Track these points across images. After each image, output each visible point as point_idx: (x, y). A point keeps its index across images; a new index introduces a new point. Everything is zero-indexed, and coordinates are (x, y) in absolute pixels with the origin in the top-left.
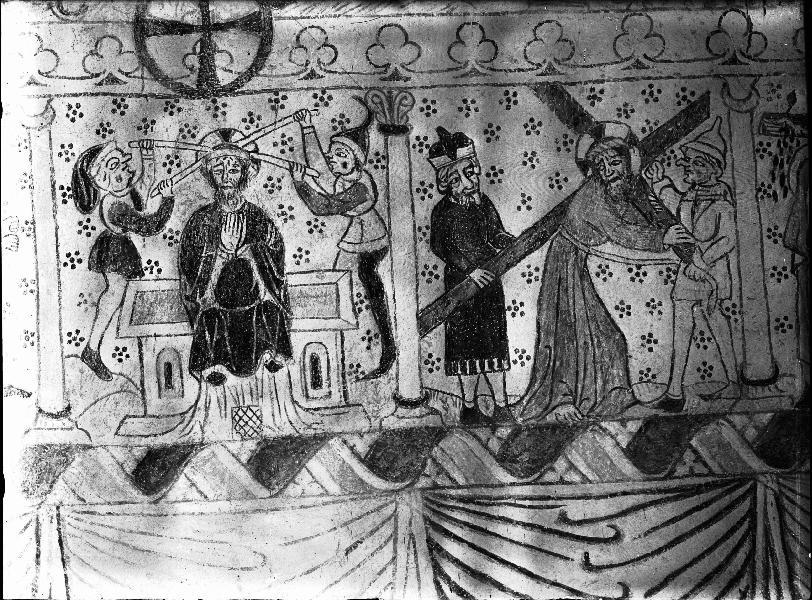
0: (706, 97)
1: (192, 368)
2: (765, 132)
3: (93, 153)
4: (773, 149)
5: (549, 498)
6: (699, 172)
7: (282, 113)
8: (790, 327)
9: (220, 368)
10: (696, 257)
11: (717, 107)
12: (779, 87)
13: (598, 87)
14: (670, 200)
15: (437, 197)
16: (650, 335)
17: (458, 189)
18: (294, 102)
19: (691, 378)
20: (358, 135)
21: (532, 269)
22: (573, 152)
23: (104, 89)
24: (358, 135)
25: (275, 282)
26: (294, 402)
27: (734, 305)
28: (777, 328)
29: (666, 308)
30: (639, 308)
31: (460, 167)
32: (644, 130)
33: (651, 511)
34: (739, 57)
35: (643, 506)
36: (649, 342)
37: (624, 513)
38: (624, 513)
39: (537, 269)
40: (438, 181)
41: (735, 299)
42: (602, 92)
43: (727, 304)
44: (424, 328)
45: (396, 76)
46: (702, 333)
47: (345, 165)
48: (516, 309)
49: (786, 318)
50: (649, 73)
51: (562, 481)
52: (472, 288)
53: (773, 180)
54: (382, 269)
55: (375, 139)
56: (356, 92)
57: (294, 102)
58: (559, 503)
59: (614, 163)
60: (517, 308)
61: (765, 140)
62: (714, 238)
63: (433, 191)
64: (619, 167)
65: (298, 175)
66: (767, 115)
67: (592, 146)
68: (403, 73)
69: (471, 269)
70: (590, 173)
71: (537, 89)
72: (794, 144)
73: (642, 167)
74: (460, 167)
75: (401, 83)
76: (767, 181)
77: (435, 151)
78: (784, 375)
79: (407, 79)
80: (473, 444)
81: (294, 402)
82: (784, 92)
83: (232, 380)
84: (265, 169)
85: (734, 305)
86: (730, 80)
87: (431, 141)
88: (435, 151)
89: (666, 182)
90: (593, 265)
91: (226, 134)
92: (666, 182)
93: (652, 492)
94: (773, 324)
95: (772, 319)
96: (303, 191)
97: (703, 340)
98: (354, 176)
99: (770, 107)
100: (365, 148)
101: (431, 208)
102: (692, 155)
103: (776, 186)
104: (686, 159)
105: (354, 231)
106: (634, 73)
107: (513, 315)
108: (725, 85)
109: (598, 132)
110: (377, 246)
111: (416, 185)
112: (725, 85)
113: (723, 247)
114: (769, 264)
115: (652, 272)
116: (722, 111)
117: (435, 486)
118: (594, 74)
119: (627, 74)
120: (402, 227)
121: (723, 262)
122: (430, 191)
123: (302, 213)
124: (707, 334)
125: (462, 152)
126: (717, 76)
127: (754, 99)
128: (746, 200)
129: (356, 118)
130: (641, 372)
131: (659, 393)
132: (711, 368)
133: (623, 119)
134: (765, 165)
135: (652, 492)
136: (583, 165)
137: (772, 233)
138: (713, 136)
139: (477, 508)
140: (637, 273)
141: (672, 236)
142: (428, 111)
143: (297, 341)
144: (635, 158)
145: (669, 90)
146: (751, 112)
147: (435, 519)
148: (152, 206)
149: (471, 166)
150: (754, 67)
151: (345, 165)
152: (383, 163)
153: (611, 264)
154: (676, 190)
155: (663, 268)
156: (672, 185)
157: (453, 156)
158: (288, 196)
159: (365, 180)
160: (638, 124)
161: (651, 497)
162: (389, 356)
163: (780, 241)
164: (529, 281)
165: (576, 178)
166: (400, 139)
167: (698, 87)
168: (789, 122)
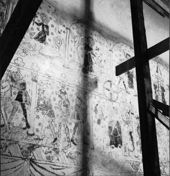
1: (110, 145)
3: (97, 105)
9: (113, 146)
20: (129, 113)
23: (99, 95)
25: (120, 133)
44: (137, 145)
54: (132, 134)
83: (115, 148)
98: (129, 119)
143: (123, 144)
148: (105, 116)
162: (134, 149)
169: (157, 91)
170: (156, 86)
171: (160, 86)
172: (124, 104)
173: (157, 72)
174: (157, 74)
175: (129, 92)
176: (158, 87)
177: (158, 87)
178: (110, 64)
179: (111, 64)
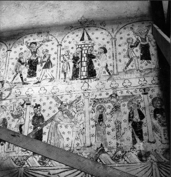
0: (81, 96)
2: (91, 102)
4: (92, 105)
5: (47, 169)
6: (79, 109)
7: (11, 103)
8: (94, 136)
10: (77, 124)
11: (82, 98)
12: (93, 94)
13: (62, 96)
14: (73, 114)
15: (34, 115)
16: (68, 138)
17: (37, 113)
18: (14, 101)
19: (75, 146)
21: (48, 127)
22: (57, 106)
24: (22, 105)
26: (4, 151)
27: (84, 132)
28: (92, 136)
29: (71, 133)
30: (66, 133)
31: (38, 110)
32: (69, 102)
33: (66, 172)
34: (86, 90)
35: (64, 171)
36: (68, 139)
37: (61, 173)
38: (61, 173)
39: (49, 126)
40: (34, 112)
41: (84, 131)
42: (63, 96)
43: (83, 132)
45: (30, 96)
46: (78, 137)
47: (19, 110)
48: (45, 134)
49: (93, 134)
50: (71, 93)
51: (50, 166)
52: (38, 130)
53: (92, 109)
54: (23, 127)
55: (25, 106)
56: (23, 99)
57: (14, 101)
58: (49, 170)
59: (64, 108)
60: (45, 133)
61: (91, 103)
62: (81, 121)
63: (33, 114)
64: (65, 109)
65: (12, 112)
66: (91, 99)
67: (61, 105)
68: (31, 95)
69: (38, 127)
70: (60, 110)
71: (53, 97)
72: (96, 104)
73: (69, 108)
74: (38, 110)
75: (31, 97)
76: (91, 110)
77: (35, 107)
78: (93, 145)
79: (31, 96)
80: (34, 159)
81: (4, 151)
82: (94, 95)
84: (7, 111)
85: (84, 132)
86: (85, 94)
87: (34, 106)
88: (35, 107)
89: (73, 111)
90: (59, 125)
91: (2, 106)
92: (73, 111)
93: (66, 168)
94: (91, 136)
95: (91, 135)
96: (12, 115)
97: (78, 139)
98: (21, 112)
99: (92, 98)
100: (23, 107)
101: (32, 117)
102: (78, 106)
103: (93, 111)
104: (77, 107)
105: (19, 122)
106: (69, 93)
107: (44, 135)
108: (84, 94)
109: (62, 103)
110: (22, 124)
111: (30, 113)
112: (84, 94)
113: (82, 122)
114: (91, 124)
115: (69, 126)
116: (83, 99)
117: (26, 167)
118: (62, 94)
119: (67, 93)
120: (27, 120)
121: (82, 125)
122: (33, 114)
123: (12, 118)
124: (79, 138)
125: (39, 107)
126: (83, 93)
127: (89, 96)
128: (87, 113)
129: (23, 102)
130: (66, 145)
131: (69, 149)
132: (79, 144)
133: (66, 101)
134: (91, 107)
135: (66, 168)
136: (59, 108)
137: (92, 119)
138: (82, 103)
139: (33, 171)
140: (66, 127)
141: (73, 120)
142: (34, 101)
144: (68, 107)
145: (74, 95)
146: (88, 99)
147: (25, 173)
149: (40, 109)
150: (89, 91)
151: (19, 110)
152: (26, 109)
153: (62, 125)
154: (74, 112)
155: (71, 126)
156: (74, 111)
157: (37, 108)
158: (10, 116)
159: (22, 113)
160: (68, 102)
161: (66, 169)
163: (93, 120)
164: (47, 129)
165: (57, 110)
166: (29, 106)
167: (79, 95)
168: (95, 100)
169: (79, 63)
170: (78, 57)
171: (85, 55)
172: (17, 98)
173: (82, 39)
174: (81, 43)
175: (27, 83)
176: (80, 58)
177: (80, 58)
178: (6, 65)
179: (7, 64)
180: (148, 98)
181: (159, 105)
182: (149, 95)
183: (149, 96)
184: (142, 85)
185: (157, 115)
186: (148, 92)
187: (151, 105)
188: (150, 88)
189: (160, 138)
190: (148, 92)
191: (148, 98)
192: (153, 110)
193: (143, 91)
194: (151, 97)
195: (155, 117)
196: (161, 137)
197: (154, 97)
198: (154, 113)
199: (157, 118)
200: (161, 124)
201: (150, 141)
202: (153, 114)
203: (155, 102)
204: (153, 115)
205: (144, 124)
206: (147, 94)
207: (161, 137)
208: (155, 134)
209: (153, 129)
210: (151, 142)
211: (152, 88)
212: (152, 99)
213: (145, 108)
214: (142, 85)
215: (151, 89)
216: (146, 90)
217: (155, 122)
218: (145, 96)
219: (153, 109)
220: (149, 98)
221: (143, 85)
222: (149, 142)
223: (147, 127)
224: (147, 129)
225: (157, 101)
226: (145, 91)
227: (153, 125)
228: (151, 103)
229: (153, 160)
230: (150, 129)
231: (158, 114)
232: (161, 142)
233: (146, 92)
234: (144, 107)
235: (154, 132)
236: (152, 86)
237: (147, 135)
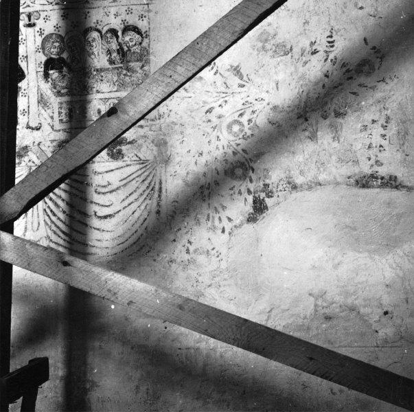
180: (35, 36)
181: (56, 50)
182: (37, 28)
183: (38, 32)
184: (25, 5)
185: (51, 72)
186: (36, 21)
187: (40, 52)
188: (41, 13)
189: (49, 120)
190: (36, 21)
191: (35, 36)
192: (43, 63)
193: (27, 19)
194: (41, 32)
195: (46, 76)
196: (52, 118)
197: (46, 33)
198: (45, 68)
199: (49, 79)
200: (55, 91)
201: (31, 125)
202: (42, 69)
203: (48, 45)
204: (42, 73)
205: (23, 91)
206: (34, 25)
207: (52, 118)
208: (43, 111)
209: (39, 102)
210: (33, 129)
211: (46, 13)
212: (43, 36)
213: (27, 57)
214: (25, 5)
215: (43, 15)
216: (32, 17)
217: (46, 88)
218: (30, 30)
219: (44, 59)
220: (37, 34)
221: (29, 6)
222: (28, 127)
223: (27, 97)
224: (27, 101)
225: (53, 42)
226: (30, 20)
227: (40, 94)
228: (40, 46)
229: (33, 162)
230: (34, 100)
231: (52, 69)
232: (52, 127)
233: (32, 21)
234: (25, 55)
235: (40, 108)
236: (46, 8)
237: (26, 114)
